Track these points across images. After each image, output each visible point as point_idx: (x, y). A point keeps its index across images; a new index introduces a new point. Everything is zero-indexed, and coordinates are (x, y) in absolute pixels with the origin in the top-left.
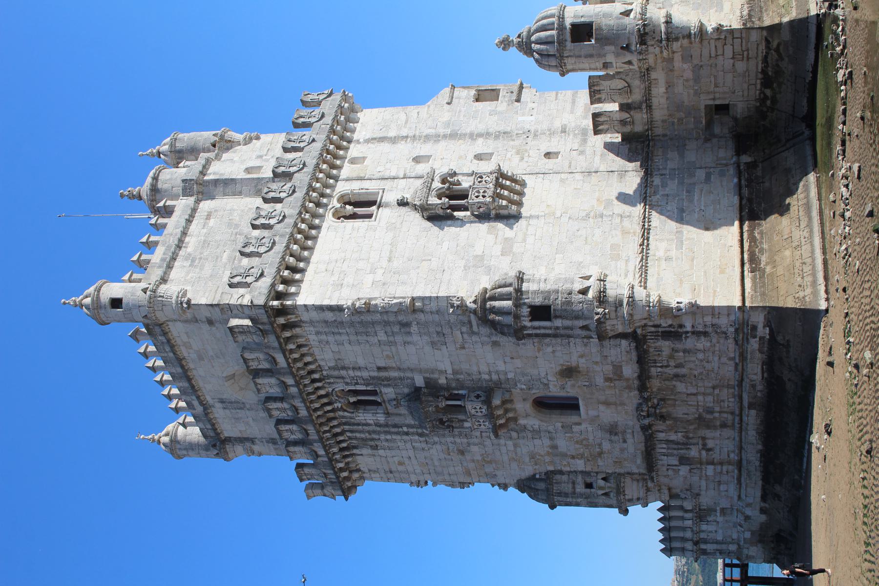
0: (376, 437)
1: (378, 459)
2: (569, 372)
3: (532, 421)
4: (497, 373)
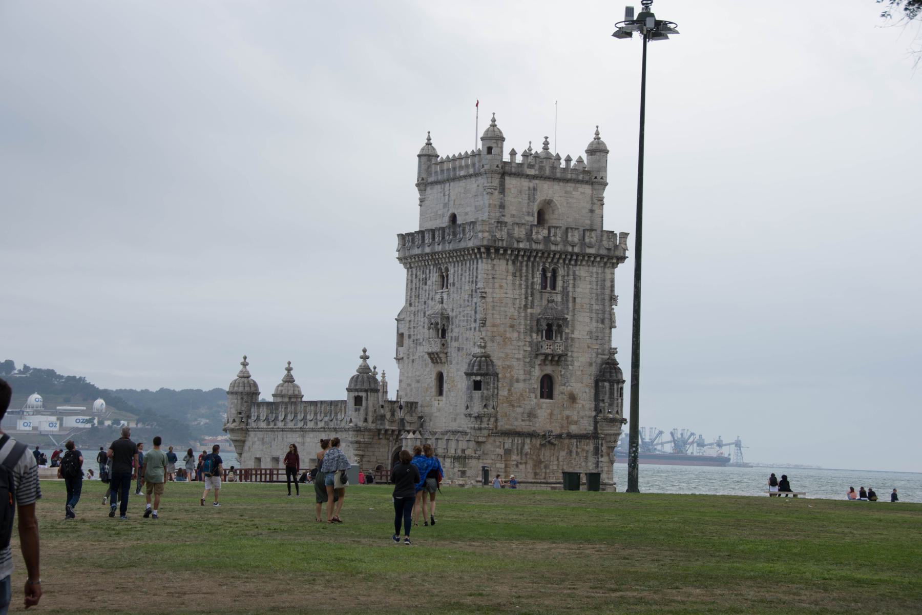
0: (524, 278)
1: (505, 274)
2: (573, 398)
3: (537, 373)
4: (573, 361)
